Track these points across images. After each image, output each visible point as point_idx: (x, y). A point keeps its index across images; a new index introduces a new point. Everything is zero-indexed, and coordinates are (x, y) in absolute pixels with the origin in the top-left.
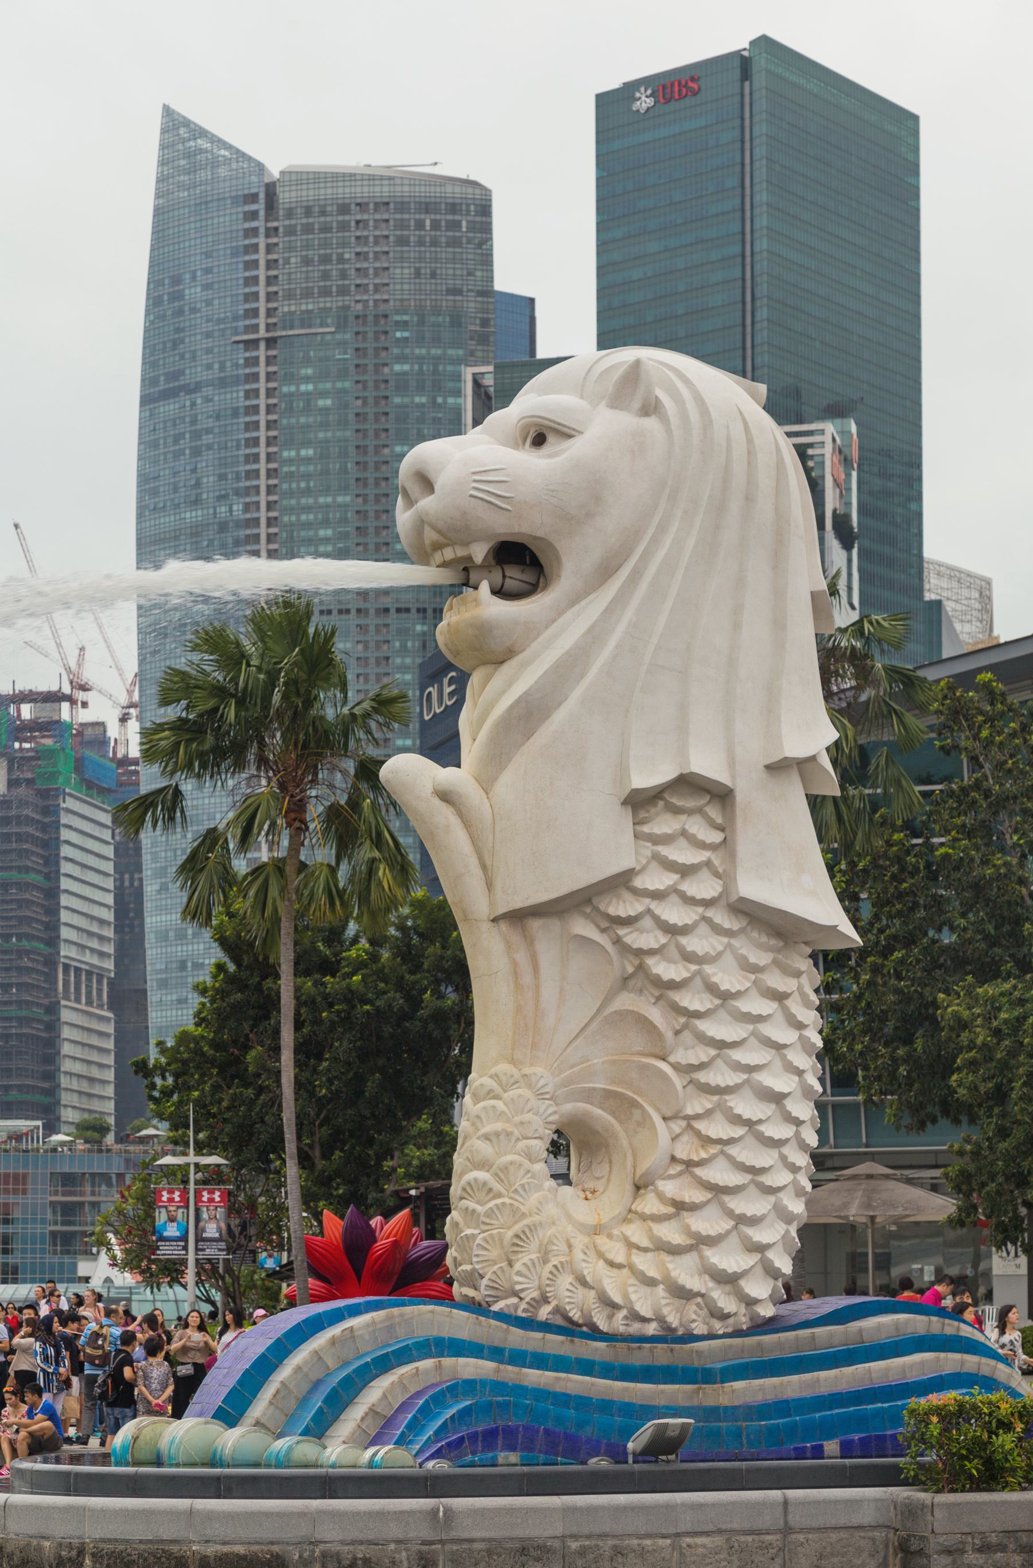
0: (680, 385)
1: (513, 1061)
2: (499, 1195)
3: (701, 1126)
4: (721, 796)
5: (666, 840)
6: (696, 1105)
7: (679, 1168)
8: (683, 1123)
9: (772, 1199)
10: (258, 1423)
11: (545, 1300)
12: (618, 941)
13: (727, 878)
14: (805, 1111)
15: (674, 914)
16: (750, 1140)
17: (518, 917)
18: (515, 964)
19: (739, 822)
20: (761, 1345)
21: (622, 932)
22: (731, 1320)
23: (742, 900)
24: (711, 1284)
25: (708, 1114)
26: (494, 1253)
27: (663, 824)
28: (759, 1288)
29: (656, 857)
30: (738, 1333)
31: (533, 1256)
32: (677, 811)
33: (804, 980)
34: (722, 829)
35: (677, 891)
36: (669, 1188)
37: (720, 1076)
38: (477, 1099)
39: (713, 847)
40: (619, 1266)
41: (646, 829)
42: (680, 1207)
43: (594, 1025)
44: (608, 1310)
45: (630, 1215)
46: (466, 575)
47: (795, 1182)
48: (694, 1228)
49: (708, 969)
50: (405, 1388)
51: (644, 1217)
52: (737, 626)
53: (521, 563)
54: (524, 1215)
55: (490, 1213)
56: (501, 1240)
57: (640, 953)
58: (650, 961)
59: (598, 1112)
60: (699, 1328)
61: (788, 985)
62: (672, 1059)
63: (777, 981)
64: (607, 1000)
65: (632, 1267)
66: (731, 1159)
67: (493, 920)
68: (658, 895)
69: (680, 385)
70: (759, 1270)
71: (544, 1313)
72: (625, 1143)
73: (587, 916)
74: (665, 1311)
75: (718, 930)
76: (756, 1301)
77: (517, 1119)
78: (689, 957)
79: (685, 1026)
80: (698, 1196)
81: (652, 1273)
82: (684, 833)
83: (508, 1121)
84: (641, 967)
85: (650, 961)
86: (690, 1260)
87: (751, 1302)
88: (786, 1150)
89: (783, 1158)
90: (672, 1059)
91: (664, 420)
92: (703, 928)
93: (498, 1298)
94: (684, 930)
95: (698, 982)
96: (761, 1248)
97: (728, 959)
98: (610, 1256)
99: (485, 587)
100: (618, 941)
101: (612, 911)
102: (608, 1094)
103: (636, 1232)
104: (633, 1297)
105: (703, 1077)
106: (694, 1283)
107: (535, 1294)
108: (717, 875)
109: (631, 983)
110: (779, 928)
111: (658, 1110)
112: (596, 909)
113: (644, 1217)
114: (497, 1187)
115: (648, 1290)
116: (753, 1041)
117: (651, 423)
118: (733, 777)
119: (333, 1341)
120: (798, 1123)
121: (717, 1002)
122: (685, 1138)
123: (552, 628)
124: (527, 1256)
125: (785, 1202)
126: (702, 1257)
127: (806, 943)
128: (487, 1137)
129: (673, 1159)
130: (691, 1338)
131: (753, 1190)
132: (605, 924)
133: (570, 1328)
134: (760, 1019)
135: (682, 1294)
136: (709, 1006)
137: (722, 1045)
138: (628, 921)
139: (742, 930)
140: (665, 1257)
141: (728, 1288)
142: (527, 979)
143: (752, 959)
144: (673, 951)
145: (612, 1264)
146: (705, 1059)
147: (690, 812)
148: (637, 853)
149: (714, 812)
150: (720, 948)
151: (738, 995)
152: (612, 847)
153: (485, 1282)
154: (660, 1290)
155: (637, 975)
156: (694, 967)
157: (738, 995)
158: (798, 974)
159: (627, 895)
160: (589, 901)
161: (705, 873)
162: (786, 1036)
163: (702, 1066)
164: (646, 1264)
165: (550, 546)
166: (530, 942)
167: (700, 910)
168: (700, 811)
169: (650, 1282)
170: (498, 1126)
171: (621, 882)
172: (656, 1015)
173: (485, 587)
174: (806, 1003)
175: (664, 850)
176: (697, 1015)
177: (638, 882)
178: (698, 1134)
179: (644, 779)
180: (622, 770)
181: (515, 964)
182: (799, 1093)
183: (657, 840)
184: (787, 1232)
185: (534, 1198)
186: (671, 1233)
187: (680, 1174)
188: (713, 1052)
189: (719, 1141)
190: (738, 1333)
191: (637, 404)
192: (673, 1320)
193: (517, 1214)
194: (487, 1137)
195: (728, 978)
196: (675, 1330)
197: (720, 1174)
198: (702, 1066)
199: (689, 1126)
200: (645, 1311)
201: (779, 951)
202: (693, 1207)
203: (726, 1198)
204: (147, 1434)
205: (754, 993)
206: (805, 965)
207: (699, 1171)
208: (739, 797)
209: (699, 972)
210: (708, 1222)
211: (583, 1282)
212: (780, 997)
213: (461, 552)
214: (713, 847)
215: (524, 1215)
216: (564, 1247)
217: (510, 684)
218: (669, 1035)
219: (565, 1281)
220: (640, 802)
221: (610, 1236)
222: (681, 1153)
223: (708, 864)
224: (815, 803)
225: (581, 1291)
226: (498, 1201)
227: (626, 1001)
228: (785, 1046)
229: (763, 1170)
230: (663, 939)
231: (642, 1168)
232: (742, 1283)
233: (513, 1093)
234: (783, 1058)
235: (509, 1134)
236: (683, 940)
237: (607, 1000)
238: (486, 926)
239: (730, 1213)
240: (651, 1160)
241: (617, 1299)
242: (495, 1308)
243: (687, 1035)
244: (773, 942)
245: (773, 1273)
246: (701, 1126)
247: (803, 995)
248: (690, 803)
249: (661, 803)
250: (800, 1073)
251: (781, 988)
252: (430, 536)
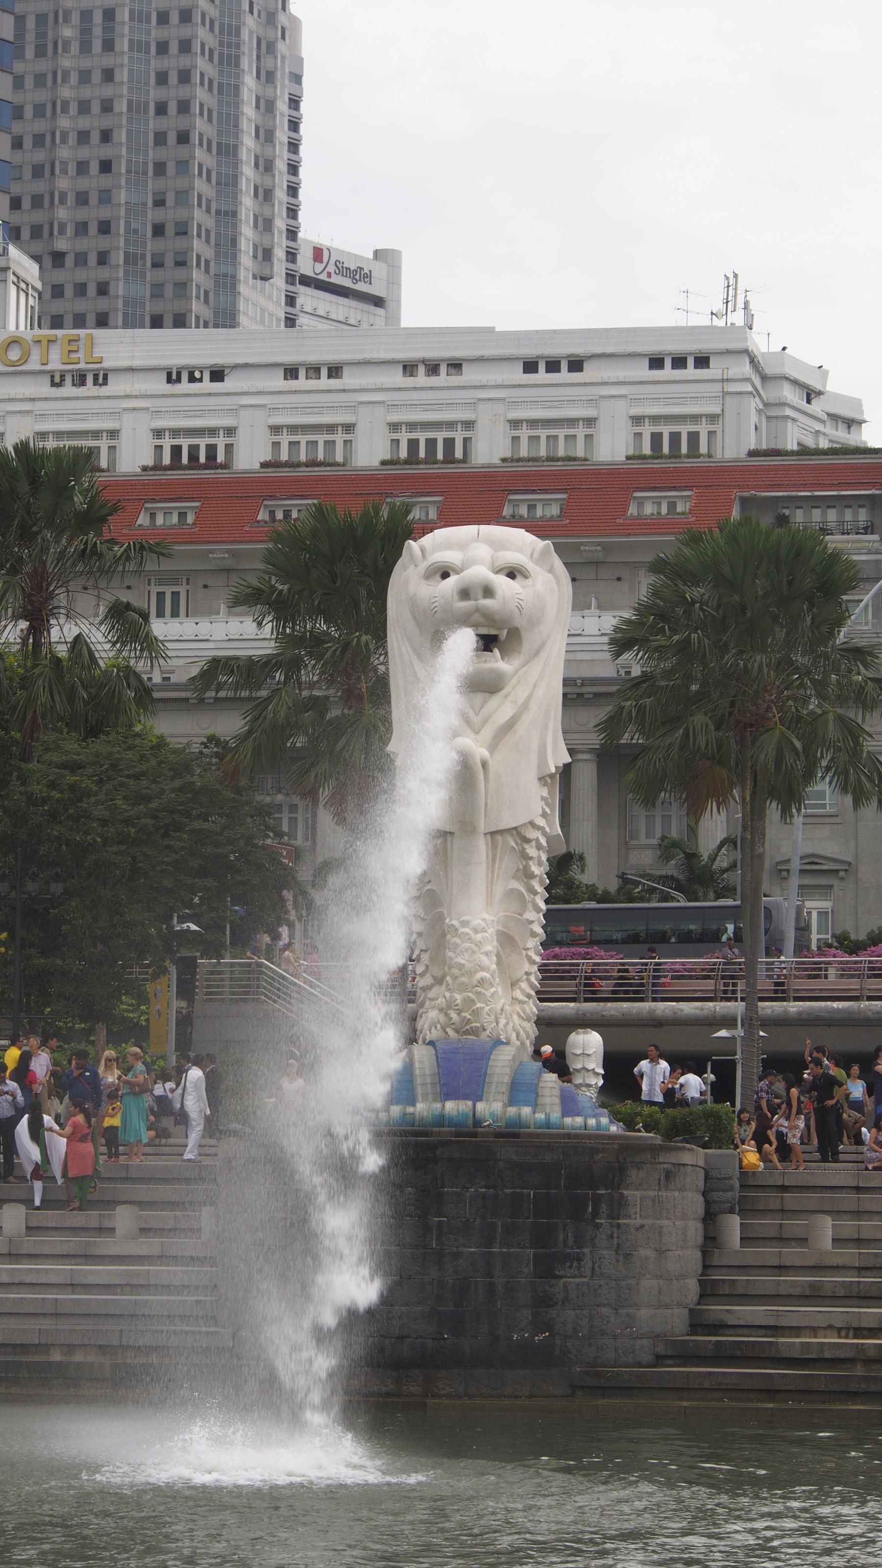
17: (492, 834)
21: (526, 846)
26: (493, 1017)
57: (531, 858)
67: (485, 834)
73: (512, 835)
138: (528, 841)
219: (514, 1035)
238: (482, 836)
252: (477, 617)
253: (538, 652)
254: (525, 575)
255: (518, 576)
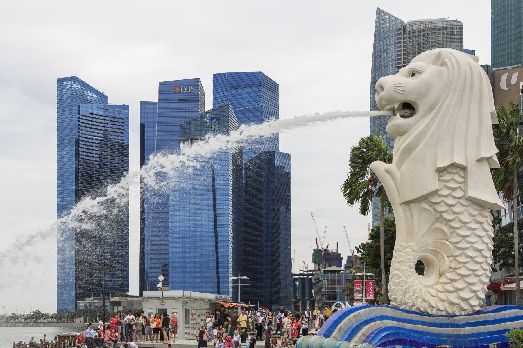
0: (452, 57)
1: (406, 242)
2: (402, 277)
3: (458, 258)
4: (464, 169)
5: (448, 181)
6: (457, 253)
7: (452, 270)
8: (453, 258)
9: (479, 278)
10: (334, 337)
11: (414, 305)
12: (434, 209)
13: (465, 191)
14: (489, 254)
15: (450, 201)
16: (472, 262)
17: (407, 203)
18: (406, 216)
19: (469, 175)
20: (476, 317)
21: (435, 206)
22: (467, 311)
23: (469, 197)
24: (461, 301)
25: (460, 255)
26: (400, 293)
27: (447, 177)
28: (475, 302)
29: (445, 186)
30: (469, 315)
31: (411, 294)
32: (451, 173)
33: (488, 218)
34: (464, 178)
35: (451, 195)
36: (449, 275)
37: (463, 245)
38: (396, 252)
39: (461, 183)
40: (435, 296)
41: (442, 178)
42: (452, 280)
43: (428, 232)
44: (431, 308)
45: (438, 283)
46: (393, 112)
47: (485, 273)
48: (456, 286)
49: (460, 216)
50: (372, 328)
51: (442, 283)
52: (468, 122)
53: (408, 108)
54: (408, 283)
55: (399, 283)
56: (402, 290)
57: (440, 212)
58: (443, 214)
59: (430, 255)
60: (457, 313)
61: (484, 220)
62: (450, 240)
63: (480, 219)
64: (432, 225)
65: (438, 297)
66: (466, 267)
67: (401, 204)
68: (445, 196)
69: (452, 57)
70: (475, 297)
71: (414, 309)
72: (437, 263)
73: (426, 203)
74: (447, 308)
75: (463, 205)
76: (474, 306)
77: (407, 257)
78: (454, 213)
79: (454, 232)
80: (457, 277)
81: (444, 298)
82: (453, 179)
83: (405, 258)
84: (441, 216)
85: (443, 214)
86: (455, 294)
87: (472, 306)
88: (482, 265)
89: (482, 267)
90: (450, 240)
91: (447, 67)
92: (458, 205)
93: (401, 305)
94: (453, 206)
95: (457, 219)
96: (475, 292)
97: (466, 213)
98: (432, 294)
99: (398, 115)
100: (434, 209)
101: (433, 201)
102: (432, 250)
103: (440, 287)
104: (438, 305)
105: (458, 245)
106: (456, 301)
107: (411, 304)
108: (462, 190)
109: (439, 220)
110: (480, 204)
111: (446, 254)
112: (428, 200)
113: (442, 283)
114: (401, 275)
115: (443, 303)
116: (473, 235)
117: (444, 68)
118: (467, 163)
119: (354, 316)
120: (486, 257)
121: (462, 225)
122: (454, 262)
123: (417, 124)
124: (410, 293)
125: (482, 279)
126: (458, 294)
127: (489, 208)
128: (398, 262)
129: (450, 267)
130: (455, 316)
131: (473, 276)
132: (431, 204)
133: (420, 313)
134: (475, 229)
135: (452, 304)
136: (460, 226)
137: (464, 236)
138: (437, 204)
139: (470, 205)
140: (447, 294)
141: (466, 302)
142: (410, 220)
143: (473, 213)
144: (450, 211)
145: (432, 296)
146: (459, 240)
147: (455, 173)
148: (440, 185)
149: (461, 173)
150: (463, 210)
151: (468, 223)
152: (432, 183)
153: (398, 301)
154: (446, 303)
155: (440, 218)
156: (456, 216)
157: (468, 223)
158: (486, 217)
159: (437, 196)
160: (427, 198)
161: (459, 190)
162: (483, 234)
163: (458, 242)
164: (443, 296)
165: (415, 103)
166: (410, 209)
167: (458, 200)
168: (457, 173)
169: (444, 301)
170: (402, 259)
171: (435, 193)
172: (445, 229)
173: (398, 115)
174: (489, 225)
175: (447, 184)
176: (457, 228)
177: (440, 193)
178: (457, 261)
179: (441, 165)
180: (436, 162)
181: (406, 216)
182: (486, 249)
183: (445, 181)
184: (483, 287)
185: (411, 279)
186: (449, 287)
187: (452, 272)
188: (461, 238)
189: (463, 263)
190: (469, 315)
191: (440, 63)
192: (450, 311)
193: (406, 283)
194: (398, 262)
195: (465, 218)
196: (450, 314)
197: (463, 271)
198: (458, 242)
199: (455, 259)
200: (443, 309)
201: (480, 210)
202: (456, 280)
203: (465, 278)
204: (306, 340)
205: (473, 222)
206: (489, 214)
207: (457, 271)
208: (468, 169)
209: (457, 217)
210: (460, 284)
211: (424, 301)
212: (481, 223)
213: (392, 106)
214: (461, 183)
215: (408, 283)
216: (419, 291)
217: (405, 141)
218: (449, 234)
219: (420, 300)
220: (440, 171)
221: (432, 288)
222: (452, 266)
223: (460, 187)
224: (492, 169)
225: (424, 303)
226: (401, 279)
227: (438, 225)
228: (482, 237)
229: (476, 270)
230: (447, 208)
231: (441, 270)
232: (470, 301)
233: (406, 250)
234: (482, 240)
235: (404, 261)
236: (453, 208)
237: (432, 225)
239: (466, 282)
240: (445, 267)
241: (434, 305)
242: (401, 308)
243: (454, 234)
244: (479, 208)
245: (479, 298)
246: (458, 258)
247: (488, 223)
248: (454, 171)
249: (446, 171)
250: (487, 244)
251: (481, 221)
253: (431, 109)
254: (420, 73)
255: (416, 74)
